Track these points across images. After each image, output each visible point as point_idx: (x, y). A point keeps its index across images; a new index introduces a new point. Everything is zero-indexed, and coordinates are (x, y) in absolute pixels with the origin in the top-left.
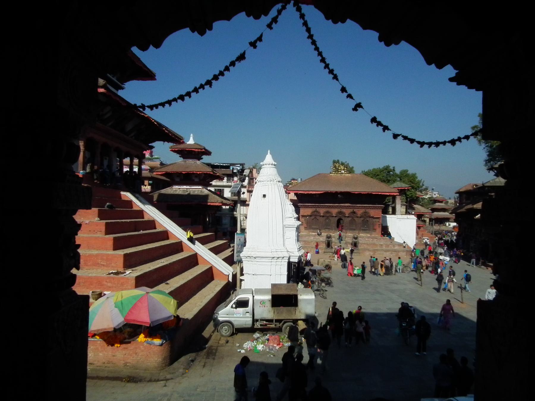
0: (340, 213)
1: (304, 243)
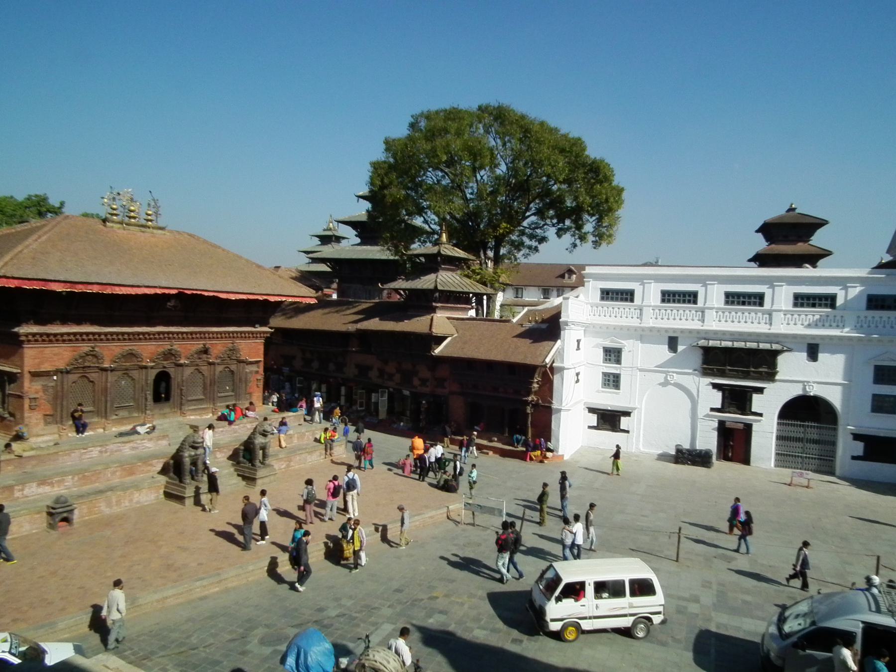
0: (169, 355)
1: (80, 479)
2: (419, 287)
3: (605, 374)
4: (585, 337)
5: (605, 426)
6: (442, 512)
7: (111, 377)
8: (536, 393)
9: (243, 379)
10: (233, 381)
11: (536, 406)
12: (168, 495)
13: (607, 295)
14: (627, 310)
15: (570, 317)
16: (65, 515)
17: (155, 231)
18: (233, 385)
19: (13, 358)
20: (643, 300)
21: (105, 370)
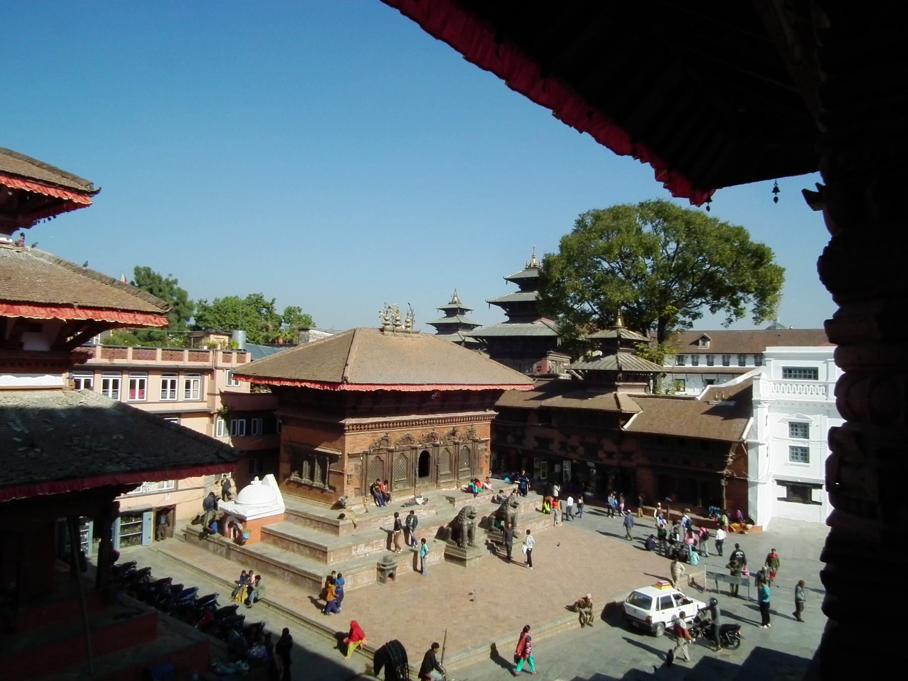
0: (431, 437)
2: (602, 368)
3: (792, 448)
4: (769, 412)
5: (795, 498)
6: (684, 579)
7: (396, 456)
8: (729, 468)
9: (477, 457)
10: (469, 458)
11: (730, 479)
12: (448, 557)
13: (789, 372)
14: (811, 386)
15: (762, 396)
16: (391, 571)
17: (413, 335)
18: (469, 461)
19: (334, 443)
20: (828, 377)
21: (391, 451)
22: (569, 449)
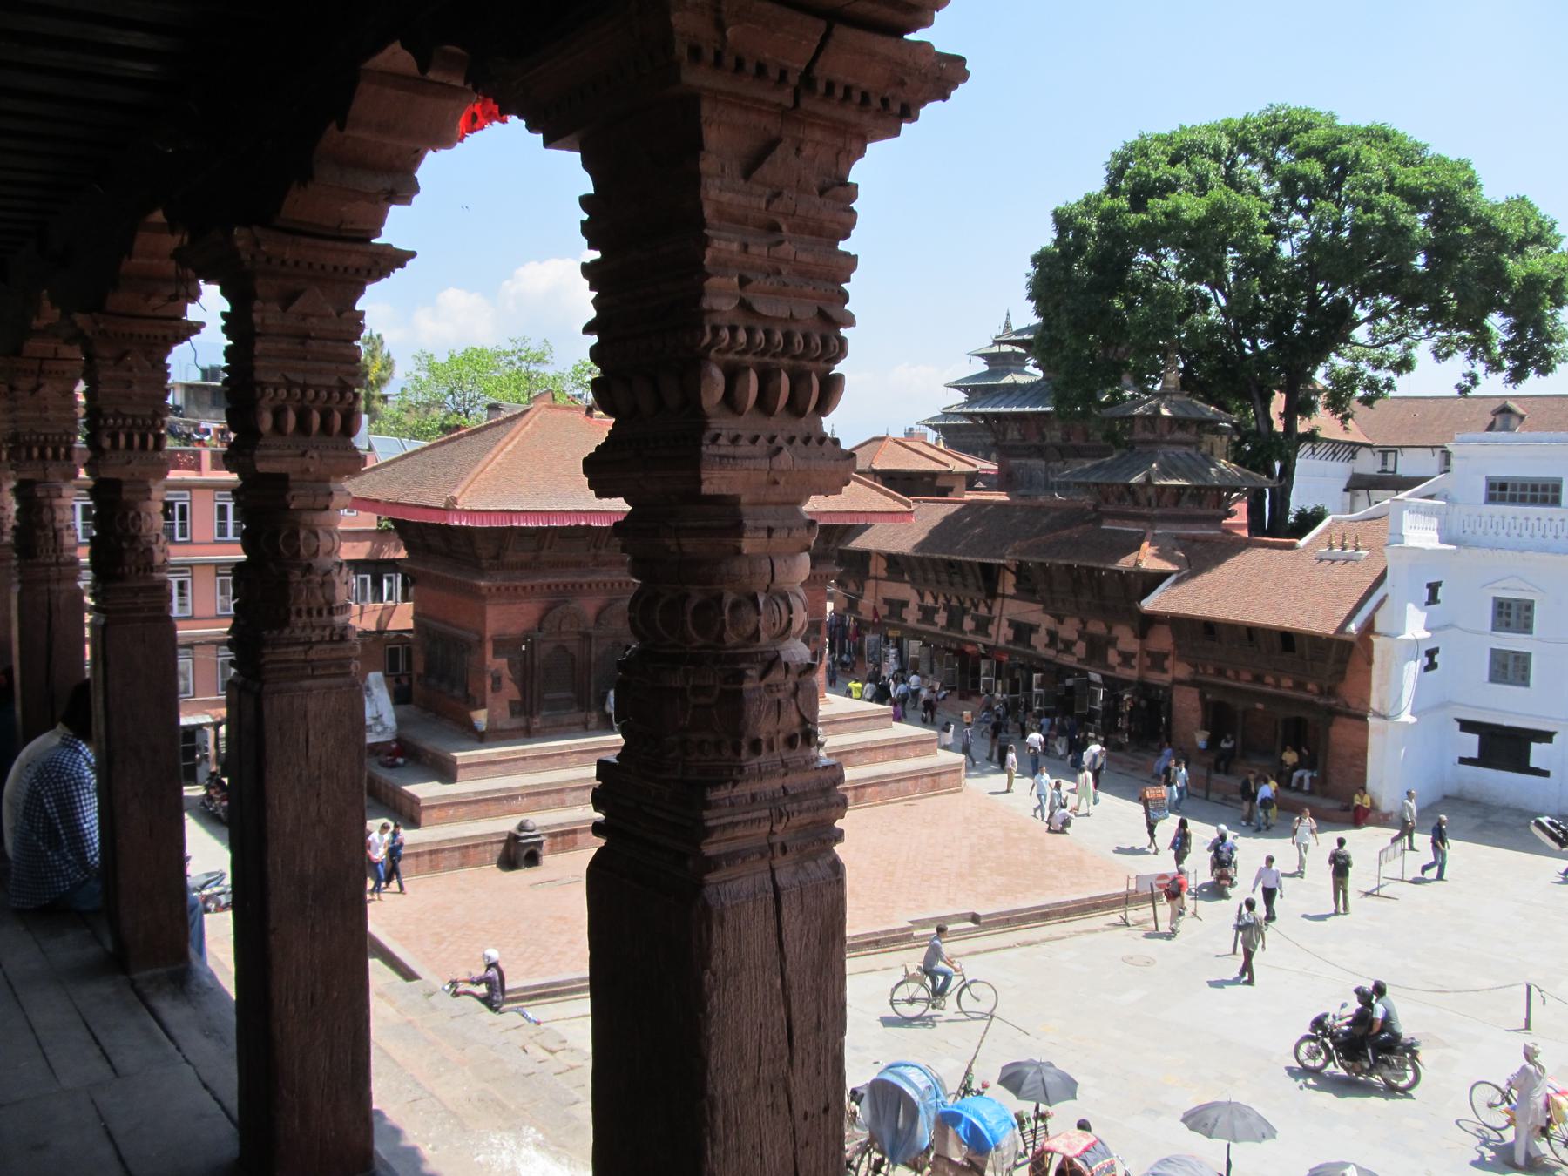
13: (1500, 491)
16: (532, 848)
22: (1061, 646)
